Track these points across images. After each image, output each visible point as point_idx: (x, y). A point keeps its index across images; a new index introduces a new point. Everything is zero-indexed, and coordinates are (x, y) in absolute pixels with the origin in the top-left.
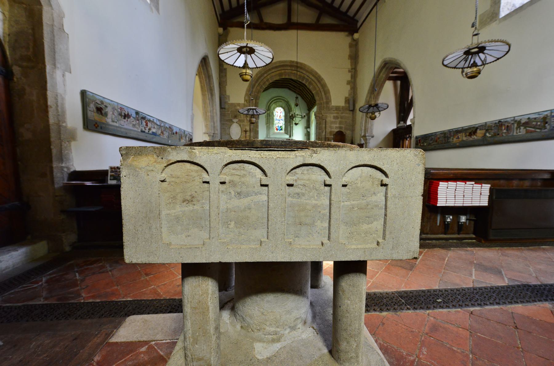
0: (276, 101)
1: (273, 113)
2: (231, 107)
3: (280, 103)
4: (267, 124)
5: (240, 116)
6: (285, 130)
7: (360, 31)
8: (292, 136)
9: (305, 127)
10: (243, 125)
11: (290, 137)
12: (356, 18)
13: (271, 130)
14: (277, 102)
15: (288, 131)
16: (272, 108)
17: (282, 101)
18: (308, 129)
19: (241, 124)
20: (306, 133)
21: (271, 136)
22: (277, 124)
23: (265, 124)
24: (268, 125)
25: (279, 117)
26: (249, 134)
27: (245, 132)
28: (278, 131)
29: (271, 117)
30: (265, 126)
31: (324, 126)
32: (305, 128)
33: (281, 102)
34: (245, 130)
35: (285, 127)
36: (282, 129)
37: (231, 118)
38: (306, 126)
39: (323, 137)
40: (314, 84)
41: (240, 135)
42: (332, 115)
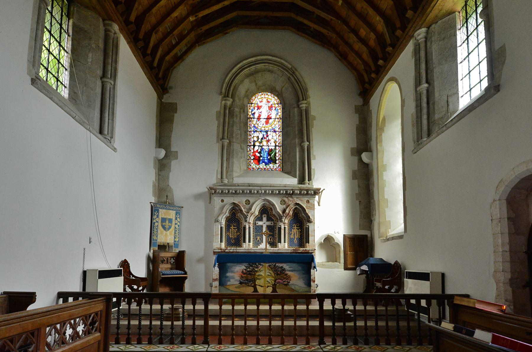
0: (253, 68)
1: (244, 109)
3: (269, 78)
4: (223, 138)
6: (283, 161)
8: (310, 179)
9: (352, 149)
11: (302, 181)
13: (235, 161)
14: (257, 72)
15: (294, 164)
16: (242, 90)
17: (275, 68)
18: (365, 157)
20: (356, 168)
21: (238, 180)
22: (257, 144)
23: (215, 139)
24: (226, 142)
25: (263, 121)
28: (262, 166)
29: (237, 120)
30: (216, 148)
32: (352, 154)
33: (271, 72)
35: (284, 152)
36: (273, 161)
38: (355, 146)
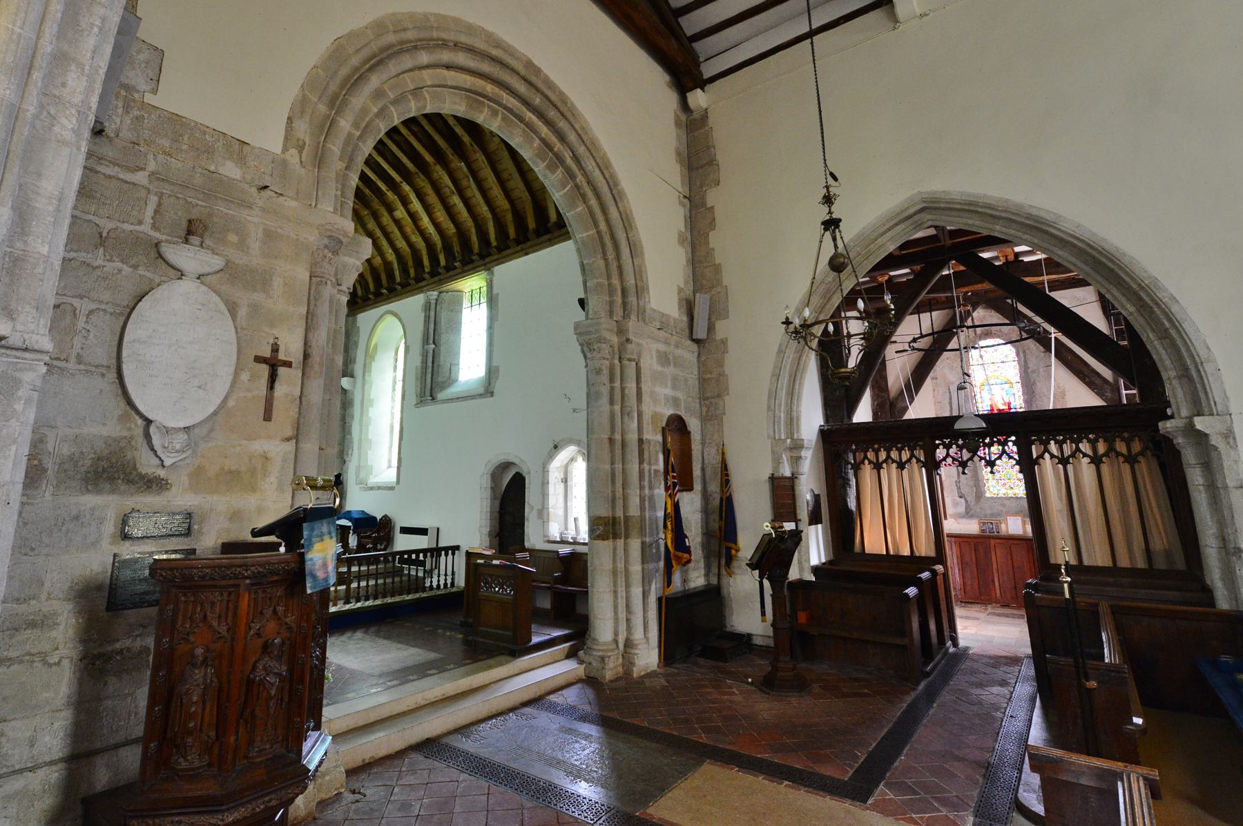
2: (166, 143)
5: (233, 238)
7: (707, 88)
10: (255, 308)
12: (698, 46)
19: (244, 298)
26: (297, 392)
27: (264, 370)
31: (631, 386)
34: (267, 353)
37: (146, 228)
39: (633, 437)
40: (593, 202)
41: (221, 387)
42: (655, 346)
